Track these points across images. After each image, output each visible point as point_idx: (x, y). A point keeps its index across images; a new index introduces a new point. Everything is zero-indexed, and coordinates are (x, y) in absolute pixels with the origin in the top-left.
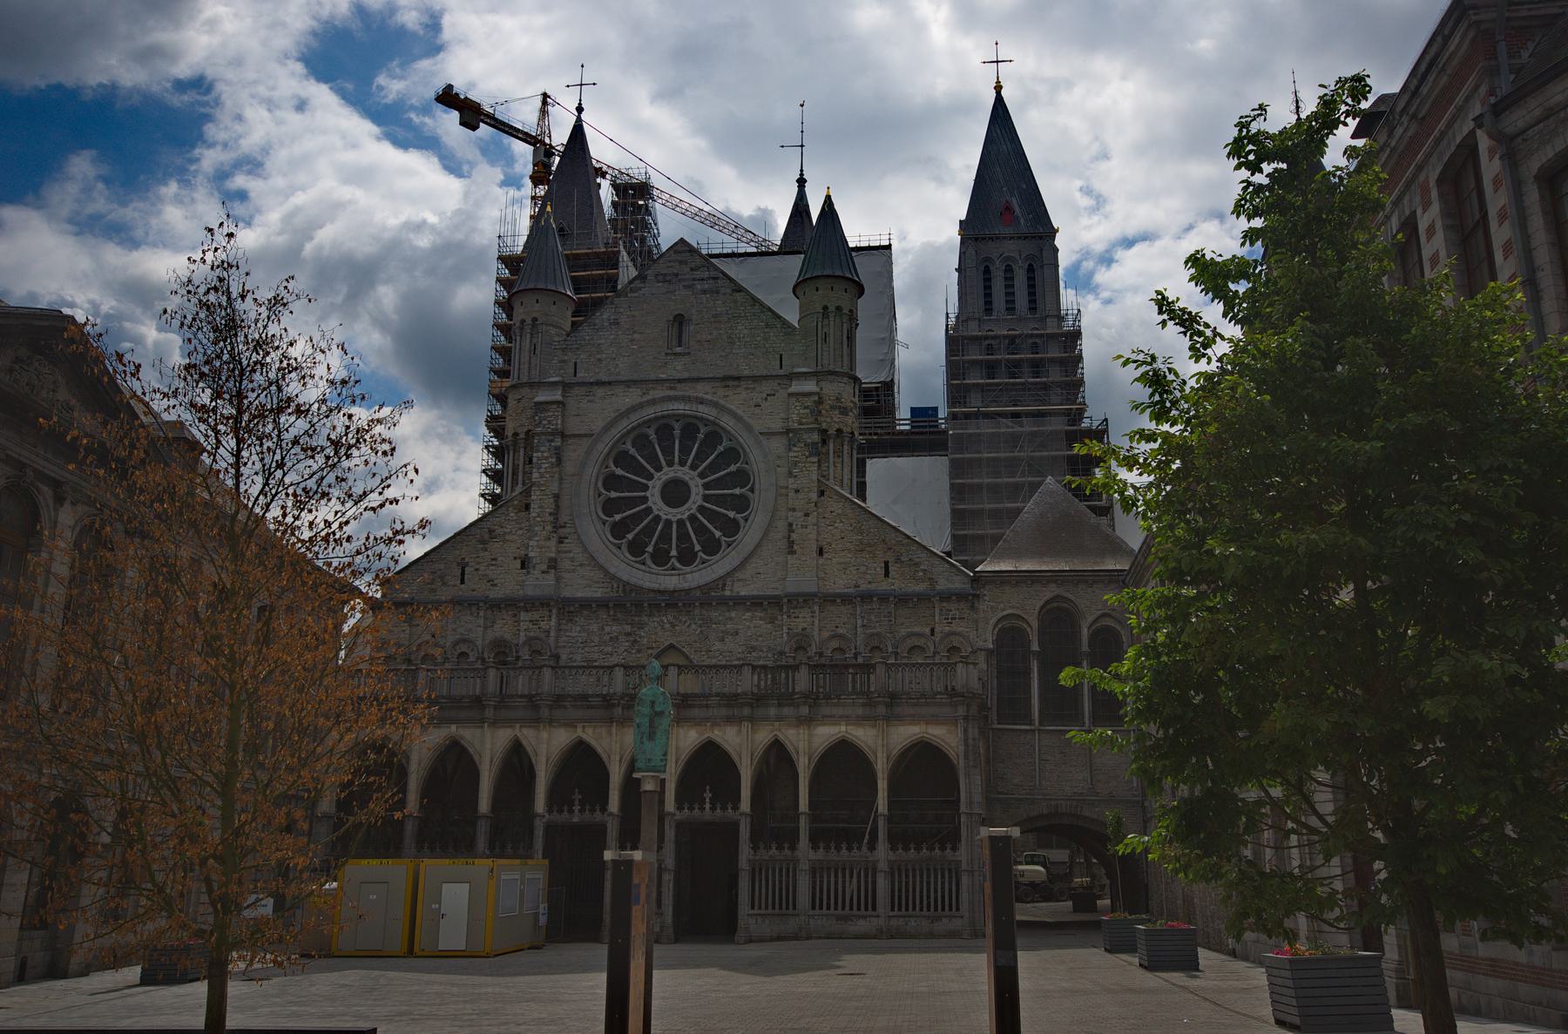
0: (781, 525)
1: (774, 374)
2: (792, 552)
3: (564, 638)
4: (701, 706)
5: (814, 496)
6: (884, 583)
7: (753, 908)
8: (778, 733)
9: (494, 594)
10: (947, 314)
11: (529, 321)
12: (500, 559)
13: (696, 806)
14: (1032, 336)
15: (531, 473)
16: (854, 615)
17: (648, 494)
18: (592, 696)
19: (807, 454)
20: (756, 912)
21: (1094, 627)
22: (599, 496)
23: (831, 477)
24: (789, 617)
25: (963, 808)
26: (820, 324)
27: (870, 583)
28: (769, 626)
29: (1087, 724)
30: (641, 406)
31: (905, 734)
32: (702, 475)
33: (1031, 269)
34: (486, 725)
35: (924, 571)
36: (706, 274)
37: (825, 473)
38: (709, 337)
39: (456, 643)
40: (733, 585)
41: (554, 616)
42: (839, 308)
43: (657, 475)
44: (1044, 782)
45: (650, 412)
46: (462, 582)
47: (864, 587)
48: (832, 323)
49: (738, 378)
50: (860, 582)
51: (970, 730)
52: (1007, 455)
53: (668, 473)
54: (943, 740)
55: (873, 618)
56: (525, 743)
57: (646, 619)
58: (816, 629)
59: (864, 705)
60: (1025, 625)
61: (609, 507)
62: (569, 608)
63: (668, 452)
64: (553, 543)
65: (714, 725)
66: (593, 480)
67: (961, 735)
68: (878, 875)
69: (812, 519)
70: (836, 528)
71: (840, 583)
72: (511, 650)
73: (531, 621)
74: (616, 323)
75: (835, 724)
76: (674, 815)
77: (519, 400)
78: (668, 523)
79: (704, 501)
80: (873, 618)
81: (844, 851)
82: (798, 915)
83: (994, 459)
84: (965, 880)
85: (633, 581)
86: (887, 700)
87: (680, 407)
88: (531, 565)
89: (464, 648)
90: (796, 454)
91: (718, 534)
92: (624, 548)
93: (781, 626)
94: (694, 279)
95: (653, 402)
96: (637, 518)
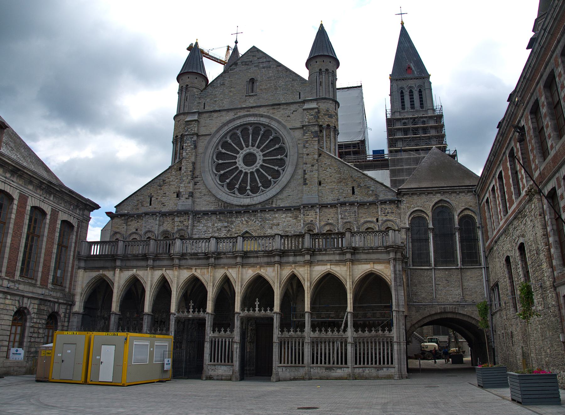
0: (300, 172)
2: (305, 184)
4: (254, 257)
5: (316, 156)
6: (352, 197)
7: (281, 363)
8: (294, 270)
9: (164, 210)
10: (386, 110)
11: (184, 86)
12: (167, 193)
13: (251, 309)
14: (422, 117)
16: (337, 213)
17: (237, 160)
19: (312, 136)
20: (282, 365)
21: (461, 215)
22: (214, 162)
23: (325, 147)
24: (304, 215)
25: (394, 308)
26: (318, 77)
27: (345, 198)
28: (295, 220)
29: (459, 265)
30: (234, 120)
31: (362, 269)
33: (420, 91)
34: (148, 268)
35: (372, 191)
36: (265, 60)
37: (321, 146)
38: (266, 87)
39: (146, 233)
40: (276, 201)
41: (190, 219)
42: (327, 70)
43: (241, 152)
44: (437, 296)
45: (238, 122)
46: (150, 205)
47: (342, 200)
48: (324, 77)
49: (279, 104)
50: (340, 197)
51: (397, 266)
53: (246, 151)
54: (382, 272)
55: (346, 214)
56: (167, 278)
57: (234, 219)
58: (318, 221)
59: (340, 254)
60: (425, 216)
61: (219, 167)
62: (198, 215)
63: (247, 142)
64: (191, 185)
65: (261, 266)
66: (211, 155)
67: (392, 268)
68: (348, 345)
69: (315, 167)
70: (328, 171)
71: (329, 199)
73: (180, 222)
74: (223, 84)
76: (240, 314)
79: (263, 162)
80: (346, 214)
81: (330, 333)
82: (305, 367)
84: (395, 347)
85: (228, 201)
86: (351, 251)
87: (252, 119)
88: (181, 195)
89: (149, 235)
90: (307, 137)
91: (270, 178)
92: (225, 186)
93: (300, 220)
94: (259, 63)
95: (240, 118)
96: (232, 172)
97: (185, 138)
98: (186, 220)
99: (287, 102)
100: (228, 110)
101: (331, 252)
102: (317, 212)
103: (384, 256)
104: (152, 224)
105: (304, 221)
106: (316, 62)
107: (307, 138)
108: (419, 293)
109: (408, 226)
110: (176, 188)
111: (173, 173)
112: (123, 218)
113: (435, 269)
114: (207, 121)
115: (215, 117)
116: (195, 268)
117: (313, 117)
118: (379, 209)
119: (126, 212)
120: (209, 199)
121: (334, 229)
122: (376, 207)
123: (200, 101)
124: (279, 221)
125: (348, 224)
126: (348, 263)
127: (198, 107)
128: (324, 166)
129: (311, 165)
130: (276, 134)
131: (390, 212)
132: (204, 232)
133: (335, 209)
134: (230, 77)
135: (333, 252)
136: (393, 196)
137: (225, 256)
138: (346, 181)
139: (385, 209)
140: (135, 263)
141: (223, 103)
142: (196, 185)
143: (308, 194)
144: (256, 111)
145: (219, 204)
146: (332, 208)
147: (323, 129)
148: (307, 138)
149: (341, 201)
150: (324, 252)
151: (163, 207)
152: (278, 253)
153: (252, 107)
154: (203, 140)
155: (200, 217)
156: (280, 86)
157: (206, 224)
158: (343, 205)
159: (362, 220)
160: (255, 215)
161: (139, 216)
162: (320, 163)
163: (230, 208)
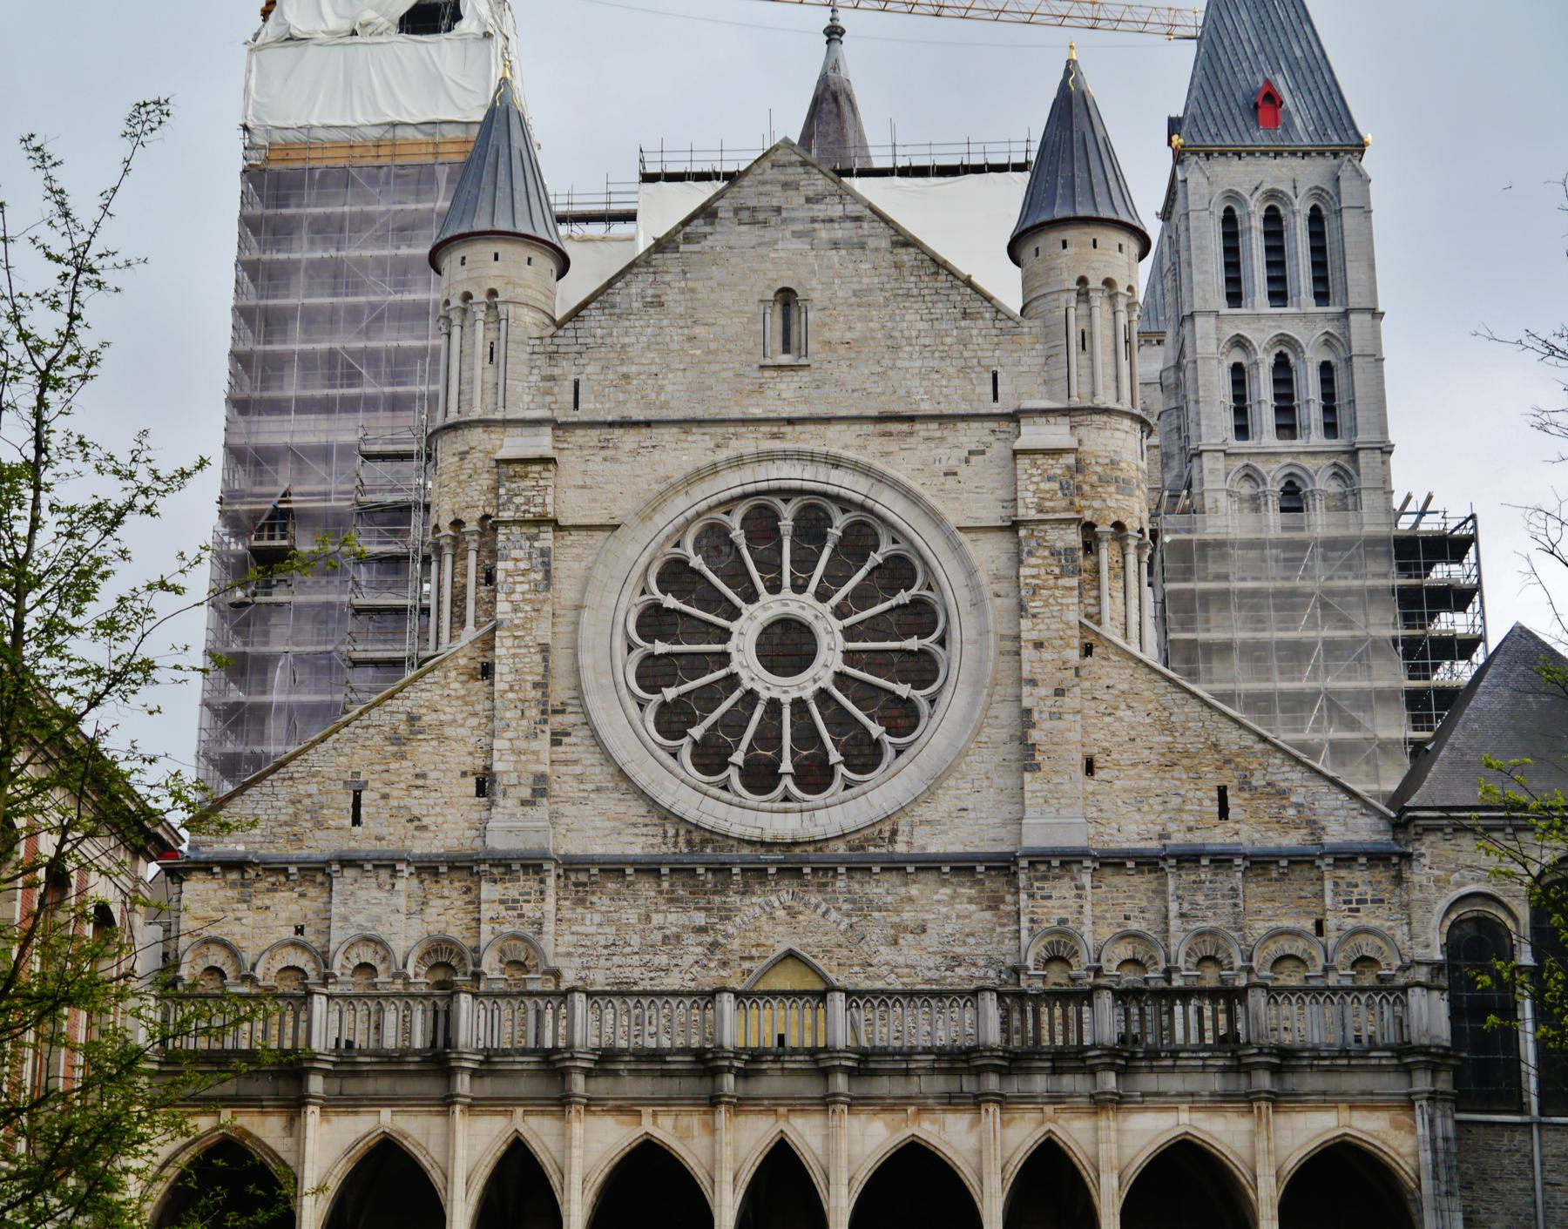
1: (983, 411)
3: (568, 938)
4: (892, 1073)
5: (1074, 655)
6: (1218, 830)
8: (1053, 1127)
9: (421, 846)
11: (480, 296)
12: (432, 775)
15: (493, 602)
16: (1161, 893)
19: (1057, 571)
24: (1031, 896)
26: (1072, 313)
27: (1190, 829)
28: (988, 915)
30: (714, 469)
34: (458, 1108)
35: (1299, 806)
36: (838, 211)
37: (1091, 610)
38: (848, 336)
40: (911, 832)
42: (1109, 283)
43: (747, 610)
45: (732, 482)
46: (356, 820)
47: (1179, 838)
49: (911, 419)
50: (1172, 827)
51: (1438, 1121)
52: (1280, 584)
53: (767, 609)
54: (1384, 1142)
55: (1200, 898)
56: (535, 1145)
57: (734, 899)
58: (1088, 920)
59: (1224, 1070)
60: (1502, 915)
63: (770, 566)
65: (923, 1109)
66: (621, 620)
67: (1422, 1130)
69: (1071, 701)
70: (1121, 719)
72: (462, 959)
73: (502, 902)
74: (657, 303)
77: (463, 455)
78: (774, 706)
80: (1200, 898)
83: (1255, 593)
85: (707, 822)
88: (499, 789)
89: (367, 955)
90: (1034, 571)
94: (814, 220)
95: (739, 462)
97: (501, 538)
99: (947, 409)
100: (686, 423)
101: (1193, 1063)
102: (1082, 888)
103: (1392, 1084)
104: (376, 910)
105: (1032, 921)
106: (1065, 245)
108: (1483, 1216)
109: (1439, 957)
110: (470, 754)
112: (233, 876)
113: (1540, 1124)
114: (592, 467)
115: (627, 447)
116: (650, 1109)
117: (1056, 486)
118: (1328, 885)
119: (241, 848)
120: (622, 808)
121: (1151, 957)
122: (1314, 874)
123: (556, 371)
125: (1208, 938)
126: (1264, 1105)
127: (549, 399)
129: (1051, 691)
130: (895, 541)
131: (1369, 897)
132: (606, 947)
133: (1153, 875)
134: (685, 273)
135: (1200, 1063)
136: (1379, 832)
137: (779, 1066)
139: (1349, 885)
140: (383, 1086)
141: (662, 388)
142: (559, 743)
143: (1045, 807)
145: (665, 832)
146: (1142, 872)
149: (1173, 841)
150: (1169, 1062)
155: (585, 885)
156: (909, 339)
157: (615, 916)
159: (1261, 924)
160: (825, 885)
161: (318, 872)
162: (1086, 684)
163: (714, 850)
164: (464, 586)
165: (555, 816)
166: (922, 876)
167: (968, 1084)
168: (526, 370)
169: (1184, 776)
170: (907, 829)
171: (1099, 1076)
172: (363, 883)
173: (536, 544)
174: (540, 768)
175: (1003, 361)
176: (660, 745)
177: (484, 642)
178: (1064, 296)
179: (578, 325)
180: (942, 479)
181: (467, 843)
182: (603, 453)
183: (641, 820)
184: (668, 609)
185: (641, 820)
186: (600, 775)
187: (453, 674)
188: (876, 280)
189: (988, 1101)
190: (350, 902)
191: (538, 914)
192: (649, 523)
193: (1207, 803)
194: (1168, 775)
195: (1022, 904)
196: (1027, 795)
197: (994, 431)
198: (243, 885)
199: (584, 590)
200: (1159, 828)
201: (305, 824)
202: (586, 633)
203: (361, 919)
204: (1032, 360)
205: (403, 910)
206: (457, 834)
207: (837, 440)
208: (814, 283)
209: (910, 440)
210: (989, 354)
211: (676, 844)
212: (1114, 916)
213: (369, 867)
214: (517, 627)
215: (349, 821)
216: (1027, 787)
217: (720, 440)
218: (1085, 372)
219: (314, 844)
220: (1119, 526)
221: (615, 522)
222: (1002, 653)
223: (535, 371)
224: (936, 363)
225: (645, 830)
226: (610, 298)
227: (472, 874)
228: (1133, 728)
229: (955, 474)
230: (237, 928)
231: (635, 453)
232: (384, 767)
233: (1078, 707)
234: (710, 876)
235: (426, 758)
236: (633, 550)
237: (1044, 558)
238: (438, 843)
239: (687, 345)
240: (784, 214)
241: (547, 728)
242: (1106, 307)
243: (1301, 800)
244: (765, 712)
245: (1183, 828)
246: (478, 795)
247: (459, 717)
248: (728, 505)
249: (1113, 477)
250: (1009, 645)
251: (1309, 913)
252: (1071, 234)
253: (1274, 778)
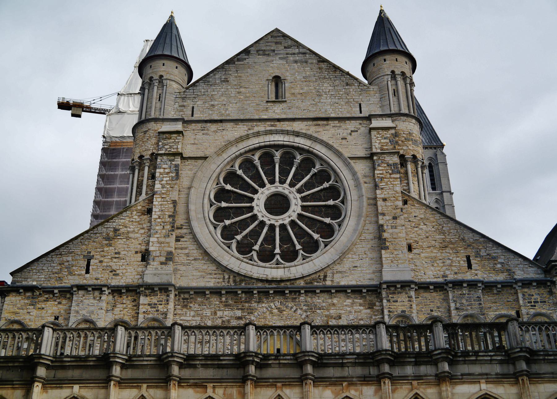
1: (355, 116)
4: (335, 365)
5: (400, 204)
6: (468, 274)
8: (418, 392)
9: (115, 282)
12: (123, 253)
16: (446, 300)
18: (223, 355)
19: (390, 172)
24: (388, 301)
26: (389, 82)
27: (456, 273)
28: (368, 311)
32: (299, 191)
35: (502, 263)
37: (405, 188)
38: (301, 91)
40: (333, 276)
45: (255, 142)
46: (87, 272)
47: (451, 277)
49: (327, 119)
50: (448, 272)
55: (464, 301)
57: (254, 305)
59: (501, 362)
66: (207, 193)
70: (422, 229)
73: (149, 305)
75: (474, 383)
80: (464, 301)
85: (243, 272)
88: (151, 258)
90: (381, 172)
94: (287, 54)
95: (258, 134)
97: (158, 160)
98: (162, 301)
99: (340, 116)
100: (236, 121)
102: (411, 297)
104: (92, 308)
105: (389, 311)
106: (385, 60)
107: (381, 174)
110: (140, 244)
111: (135, 217)
112: (28, 294)
114: (197, 136)
115: (212, 130)
116: (212, 385)
117: (388, 141)
119: (35, 283)
120: (205, 267)
122: (513, 291)
123: (185, 104)
124: (341, 312)
128: (414, 220)
129: (391, 218)
131: (539, 300)
133: (442, 293)
134: (237, 71)
135: (489, 358)
136: (538, 274)
137: (277, 362)
138: (456, 246)
139: (529, 295)
140: (76, 374)
141: (227, 109)
142: (179, 241)
143: (392, 264)
144: (286, 126)
145: (224, 277)
146: (437, 291)
147: (407, 161)
148: (381, 174)
150: (474, 358)
151: (114, 277)
152: (389, 357)
153: (279, 120)
154: (192, 167)
155: (187, 299)
156: (325, 92)
157: (200, 312)
158: (457, 287)
160: (295, 298)
162: (406, 215)
163: (246, 284)
164: (142, 181)
165: (175, 270)
166: (338, 295)
167: (373, 371)
168: (173, 103)
169: (451, 252)
170: (331, 275)
171: (440, 365)
172: (87, 296)
173: (173, 163)
174: (169, 249)
175: (363, 100)
176: (223, 242)
177: (149, 200)
178: (386, 77)
179: (194, 88)
180: (341, 141)
181: (136, 281)
182: (203, 132)
183: (214, 272)
184: (227, 190)
185: (214, 272)
186: (196, 253)
187: (135, 213)
188: (312, 73)
189: (385, 378)
190: (80, 305)
191: (165, 310)
192: (220, 157)
193: (462, 262)
194: (444, 251)
195: (384, 304)
196: (384, 259)
197: (361, 124)
198: (33, 298)
199: (192, 181)
200: (443, 273)
201: (64, 273)
202: (193, 197)
203: (84, 313)
204: (375, 99)
205: (104, 308)
206: (132, 277)
207: (297, 126)
208: (288, 74)
209: (327, 127)
210: (358, 97)
211: (229, 282)
212: (426, 310)
213: (90, 289)
214: (163, 193)
215: (84, 272)
216: (383, 256)
217: (250, 127)
218: (396, 103)
219: (67, 281)
220: (414, 157)
221: (207, 156)
222: (369, 205)
223: (177, 104)
224: (337, 101)
225: (215, 276)
226: (208, 79)
227: (137, 294)
228: (427, 233)
229: (346, 139)
230: (28, 317)
231: (215, 132)
232: (102, 250)
233: (403, 224)
234: (243, 295)
235: (120, 246)
236: (213, 167)
237: (385, 167)
238: (122, 281)
239: (237, 95)
240: (276, 52)
241: (174, 233)
242: (402, 82)
243: (503, 261)
244: (268, 230)
245: (452, 273)
246: (142, 261)
247: (136, 230)
248: (253, 151)
249: (409, 137)
250: (371, 202)
251: (513, 308)
252: (387, 57)
253: (490, 252)
